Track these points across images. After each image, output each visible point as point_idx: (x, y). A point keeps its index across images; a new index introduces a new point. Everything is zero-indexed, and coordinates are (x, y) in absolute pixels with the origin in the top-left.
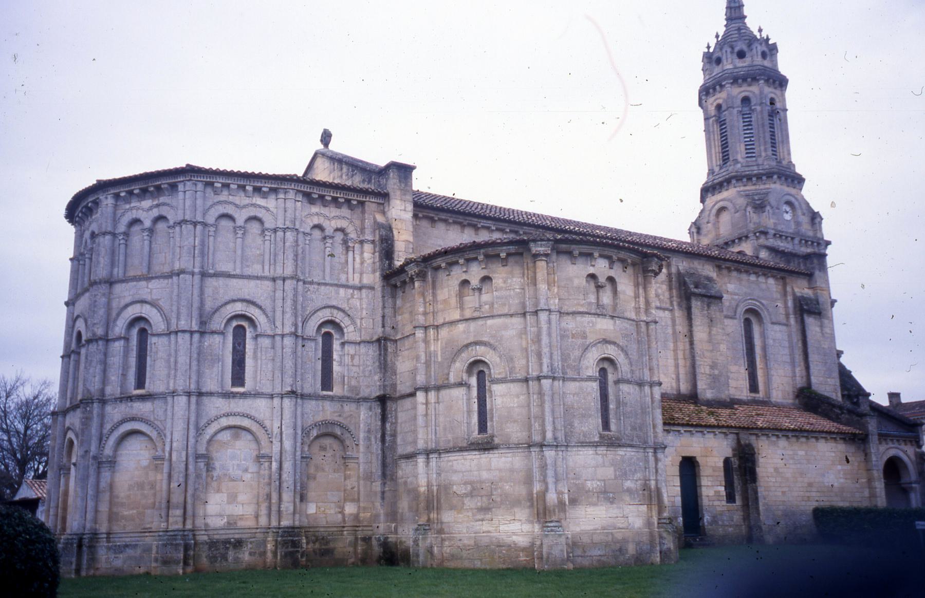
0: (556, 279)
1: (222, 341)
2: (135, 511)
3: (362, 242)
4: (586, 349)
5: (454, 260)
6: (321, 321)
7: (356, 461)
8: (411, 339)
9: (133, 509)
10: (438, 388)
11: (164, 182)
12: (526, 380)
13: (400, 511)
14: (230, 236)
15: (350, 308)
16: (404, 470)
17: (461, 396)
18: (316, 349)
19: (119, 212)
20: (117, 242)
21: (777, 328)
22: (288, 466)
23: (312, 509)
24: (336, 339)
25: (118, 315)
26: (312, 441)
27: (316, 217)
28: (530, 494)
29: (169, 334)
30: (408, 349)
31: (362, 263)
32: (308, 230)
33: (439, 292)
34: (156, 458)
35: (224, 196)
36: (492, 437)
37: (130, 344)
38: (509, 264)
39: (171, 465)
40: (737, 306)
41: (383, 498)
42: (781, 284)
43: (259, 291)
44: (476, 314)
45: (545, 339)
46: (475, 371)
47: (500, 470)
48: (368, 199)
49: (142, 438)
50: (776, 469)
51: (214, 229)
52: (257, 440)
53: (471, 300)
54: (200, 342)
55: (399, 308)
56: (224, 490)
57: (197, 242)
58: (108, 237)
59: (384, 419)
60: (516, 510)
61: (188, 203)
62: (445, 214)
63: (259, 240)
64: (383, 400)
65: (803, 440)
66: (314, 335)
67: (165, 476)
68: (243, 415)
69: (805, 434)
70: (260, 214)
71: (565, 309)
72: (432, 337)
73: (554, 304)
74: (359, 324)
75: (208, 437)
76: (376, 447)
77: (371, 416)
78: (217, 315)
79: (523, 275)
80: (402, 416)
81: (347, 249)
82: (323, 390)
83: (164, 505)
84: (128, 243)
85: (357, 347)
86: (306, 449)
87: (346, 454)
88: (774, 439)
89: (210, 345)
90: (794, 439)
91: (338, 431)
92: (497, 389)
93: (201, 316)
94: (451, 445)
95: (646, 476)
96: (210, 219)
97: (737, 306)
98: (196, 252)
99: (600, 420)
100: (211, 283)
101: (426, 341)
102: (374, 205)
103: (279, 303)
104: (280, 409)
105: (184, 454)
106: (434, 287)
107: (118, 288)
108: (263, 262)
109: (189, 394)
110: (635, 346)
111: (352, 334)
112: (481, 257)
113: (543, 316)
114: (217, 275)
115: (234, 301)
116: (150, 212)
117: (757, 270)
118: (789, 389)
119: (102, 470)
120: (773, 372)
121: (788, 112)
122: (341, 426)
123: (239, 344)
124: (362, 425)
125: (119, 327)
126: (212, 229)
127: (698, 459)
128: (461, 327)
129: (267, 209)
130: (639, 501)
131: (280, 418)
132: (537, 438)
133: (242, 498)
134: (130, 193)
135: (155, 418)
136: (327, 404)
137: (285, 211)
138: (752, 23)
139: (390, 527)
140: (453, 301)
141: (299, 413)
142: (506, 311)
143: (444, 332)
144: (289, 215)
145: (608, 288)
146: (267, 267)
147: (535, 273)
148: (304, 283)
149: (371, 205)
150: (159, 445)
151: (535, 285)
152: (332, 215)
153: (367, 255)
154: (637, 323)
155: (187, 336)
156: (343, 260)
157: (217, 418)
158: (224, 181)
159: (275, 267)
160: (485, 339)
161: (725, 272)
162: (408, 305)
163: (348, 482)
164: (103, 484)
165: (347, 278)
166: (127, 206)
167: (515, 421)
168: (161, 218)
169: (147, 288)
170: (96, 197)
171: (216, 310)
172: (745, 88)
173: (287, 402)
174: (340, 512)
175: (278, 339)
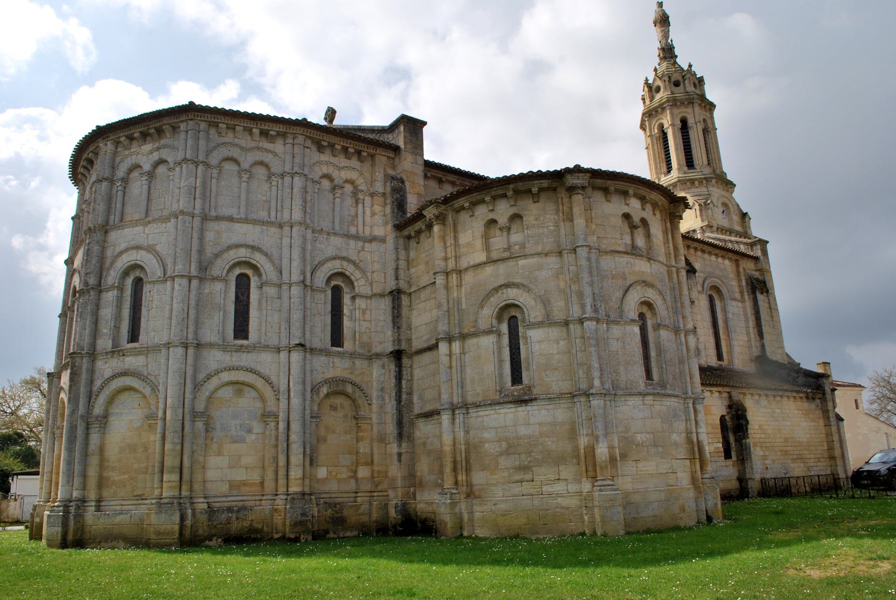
0: (593, 215)
1: (224, 288)
2: (126, 476)
3: (372, 195)
5: (479, 198)
6: (331, 273)
9: (124, 473)
10: (463, 337)
13: (418, 474)
14: (235, 180)
15: (361, 261)
16: (423, 429)
17: (492, 346)
18: (325, 303)
19: (118, 159)
20: (115, 189)
21: (734, 303)
22: (295, 426)
23: (322, 473)
24: (347, 293)
26: (321, 401)
28: (576, 449)
30: (425, 301)
32: (317, 178)
34: (148, 417)
35: (229, 137)
37: (124, 295)
38: (542, 200)
41: (400, 460)
42: (735, 265)
44: (506, 254)
46: (506, 317)
47: (540, 424)
48: (378, 151)
49: (136, 396)
52: (262, 399)
53: (498, 241)
54: (199, 288)
55: (413, 260)
56: (225, 453)
59: (399, 377)
62: (452, 176)
63: (265, 186)
64: (397, 355)
66: (324, 286)
67: (158, 436)
70: (268, 158)
73: (593, 240)
74: (370, 278)
75: (207, 393)
76: (390, 406)
77: (384, 374)
79: (557, 211)
80: (417, 373)
82: (332, 345)
84: (127, 190)
85: (369, 301)
86: (316, 408)
87: (358, 414)
91: (349, 389)
92: (535, 335)
93: (200, 262)
94: (480, 398)
96: (214, 160)
98: (197, 193)
101: (447, 287)
103: (286, 251)
104: (287, 364)
105: (180, 411)
108: (269, 209)
113: (582, 253)
115: (238, 246)
116: (151, 156)
117: (717, 251)
120: (735, 343)
121: (717, 131)
122: (353, 384)
123: (243, 295)
124: (375, 384)
128: (489, 270)
130: (684, 455)
131: (287, 374)
132: (584, 386)
133: (246, 460)
134: (131, 138)
135: (148, 373)
136: (337, 361)
137: (293, 157)
139: (408, 493)
140: (479, 243)
141: (308, 367)
142: (539, 249)
143: (468, 278)
146: (273, 213)
147: (571, 209)
148: (313, 231)
150: (153, 402)
151: (572, 220)
152: (342, 165)
153: (377, 208)
156: (353, 212)
157: (217, 372)
159: (282, 214)
160: (518, 280)
162: (424, 255)
163: (361, 444)
165: (357, 230)
166: (127, 152)
167: (555, 369)
168: (162, 161)
169: (144, 233)
171: (217, 256)
174: (352, 477)
175: (285, 287)
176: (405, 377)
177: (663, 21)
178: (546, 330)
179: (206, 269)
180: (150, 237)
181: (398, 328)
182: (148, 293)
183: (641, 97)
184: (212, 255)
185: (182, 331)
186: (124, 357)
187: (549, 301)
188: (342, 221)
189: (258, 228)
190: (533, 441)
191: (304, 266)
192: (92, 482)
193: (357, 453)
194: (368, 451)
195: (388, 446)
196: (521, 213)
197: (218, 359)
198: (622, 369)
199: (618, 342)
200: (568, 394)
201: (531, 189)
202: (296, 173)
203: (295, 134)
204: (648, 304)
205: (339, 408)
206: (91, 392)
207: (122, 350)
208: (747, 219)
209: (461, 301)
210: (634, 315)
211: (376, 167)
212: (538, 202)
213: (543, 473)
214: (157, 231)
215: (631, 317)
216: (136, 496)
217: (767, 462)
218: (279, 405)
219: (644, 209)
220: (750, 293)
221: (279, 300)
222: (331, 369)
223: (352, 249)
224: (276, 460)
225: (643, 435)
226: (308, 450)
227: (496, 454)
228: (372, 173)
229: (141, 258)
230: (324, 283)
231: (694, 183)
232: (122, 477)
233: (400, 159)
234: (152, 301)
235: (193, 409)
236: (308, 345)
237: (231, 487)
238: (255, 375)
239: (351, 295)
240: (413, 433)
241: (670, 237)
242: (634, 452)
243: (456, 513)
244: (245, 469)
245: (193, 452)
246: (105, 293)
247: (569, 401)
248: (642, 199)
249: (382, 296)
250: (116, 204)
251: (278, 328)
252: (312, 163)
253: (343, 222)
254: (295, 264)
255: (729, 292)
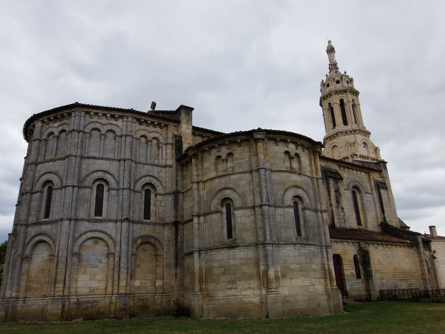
0: (268, 152)
1: (90, 192)
2: (39, 285)
3: (166, 144)
4: (286, 191)
5: (212, 145)
6: (144, 183)
7: (162, 257)
8: (191, 191)
9: (38, 284)
10: (205, 215)
11: (65, 112)
12: (254, 207)
13: (185, 284)
14: (98, 139)
15: (160, 177)
17: (217, 219)
18: (141, 198)
19: (43, 130)
20: (41, 145)
21: (367, 195)
22: (123, 259)
23: (137, 283)
24: (153, 193)
25: (38, 180)
27: (143, 131)
28: (259, 272)
29: (61, 188)
30: (189, 196)
31: (166, 155)
32: (139, 137)
33: (205, 164)
34: (51, 256)
35: (95, 119)
36: (235, 240)
37: (43, 195)
38: (242, 146)
39: (58, 259)
40: (349, 184)
41: (176, 277)
42: (368, 175)
43: (112, 167)
44: (225, 173)
45: (263, 184)
46: (225, 204)
47: (240, 259)
48: (169, 123)
49: (46, 245)
50: (379, 261)
51: (89, 135)
53: (221, 167)
54: (78, 192)
56: (88, 273)
57: (79, 140)
58: (37, 142)
59: (177, 234)
60: (251, 282)
61: (76, 121)
62: (209, 134)
63: (113, 142)
64: (176, 224)
65: (390, 246)
67: (55, 265)
68: (100, 231)
69: (391, 243)
70: (114, 128)
71: (274, 169)
72: (201, 188)
73: (267, 166)
74: (164, 185)
75: (80, 243)
76: (172, 249)
77: (171, 232)
78: (88, 178)
79: (250, 151)
80: (186, 232)
81: (159, 148)
82: (144, 219)
83: (53, 282)
84: (47, 145)
85: (163, 197)
86: (135, 250)
87: (157, 253)
88: (376, 245)
89: (84, 194)
90: (386, 246)
91: (152, 241)
92: (238, 213)
93: (79, 179)
94: (212, 245)
95: (322, 262)
96: (88, 130)
97: (349, 184)
98: (79, 146)
99: (296, 230)
100: (86, 161)
101: (198, 190)
102: (173, 126)
103: (122, 173)
104: (120, 229)
106: (202, 162)
107: (39, 167)
108: (115, 152)
109: (70, 220)
110: (311, 191)
111: (160, 190)
112: (227, 143)
113: (262, 171)
114: (89, 158)
115: (98, 171)
117: (357, 168)
118: (375, 224)
119: (24, 262)
120: (368, 216)
121: (360, 105)
122: (155, 238)
124: (165, 238)
125: (38, 187)
126: (88, 135)
127: (341, 256)
128: (217, 181)
129: (118, 126)
131: (120, 233)
133: (99, 277)
135: (52, 233)
136: (146, 226)
137: (127, 127)
138: (341, 71)
140: (212, 167)
141: (131, 230)
142: (241, 170)
143: (208, 185)
144: (129, 129)
145: (296, 159)
146: (116, 155)
147: (257, 149)
148: (136, 163)
149: (171, 127)
150: (53, 247)
151: (257, 155)
152: (151, 131)
153: (169, 151)
154: (312, 178)
155: (71, 189)
156: (157, 153)
157: (85, 233)
158: (95, 111)
159: (120, 155)
160: (230, 186)
161: (342, 168)
162: (189, 173)
164: (23, 271)
166: (48, 127)
167: (248, 231)
169: (53, 165)
170: (34, 123)
171: (87, 176)
172: (341, 95)
173: (125, 224)
174: (153, 285)
175: (121, 191)
176: (180, 234)
177: (331, 50)
178: (244, 211)
179: (82, 182)
180: (56, 167)
181: (177, 210)
182: (54, 194)
183: (320, 90)
184: (85, 175)
185: (68, 212)
186: (41, 226)
187: (245, 196)
188: (151, 157)
189: (108, 162)
190: (237, 268)
191: (130, 180)
192: (23, 288)
193: (156, 273)
194: (161, 272)
195: (171, 269)
196: (232, 152)
197: (86, 226)
198: (283, 231)
199: (281, 217)
200: (254, 243)
201: (237, 140)
202: (127, 135)
203: (127, 116)
204: (298, 197)
205: (147, 250)
206: (25, 243)
207: (40, 222)
208: (378, 151)
209: (204, 196)
210: (291, 203)
211: (169, 131)
212: (241, 146)
213: (242, 284)
214: (59, 164)
215: (288, 204)
216: (42, 295)
217: (383, 281)
218: (115, 249)
219: (297, 149)
220: (376, 190)
221: (118, 197)
222: (143, 231)
223: (155, 171)
224: (113, 276)
225: (295, 265)
226: (129, 272)
227: (219, 274)
228: (167, 134)
229: (52, 177)
230: (141, 188)
231: (347, 132)
232: (37, 286)
233: (180, 126)
234: (55, 198)
235: (73, 251)
236: (131, 219)
237: (90, 290)
238: (104, 234)
239: (155, 194)
240: (183, 263)
241: (313, 162)
242: (289, 274)
243: (200, 305)
244: (97, 281)
245: (71, 273)
246: (34, 194)
247: (255, 247)
248: (295, 143)
249: (169, 194)
250: (42, 151)
251: (116, 210)
252: (136, 130)
253: (152, 158)
254: (126, 179)
255: (364, 189)
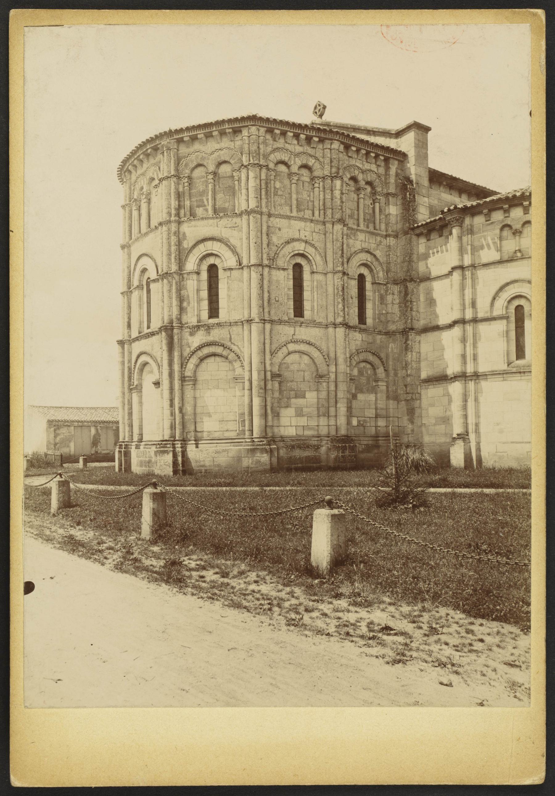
70: (311, 162)
146: (317, 213)
